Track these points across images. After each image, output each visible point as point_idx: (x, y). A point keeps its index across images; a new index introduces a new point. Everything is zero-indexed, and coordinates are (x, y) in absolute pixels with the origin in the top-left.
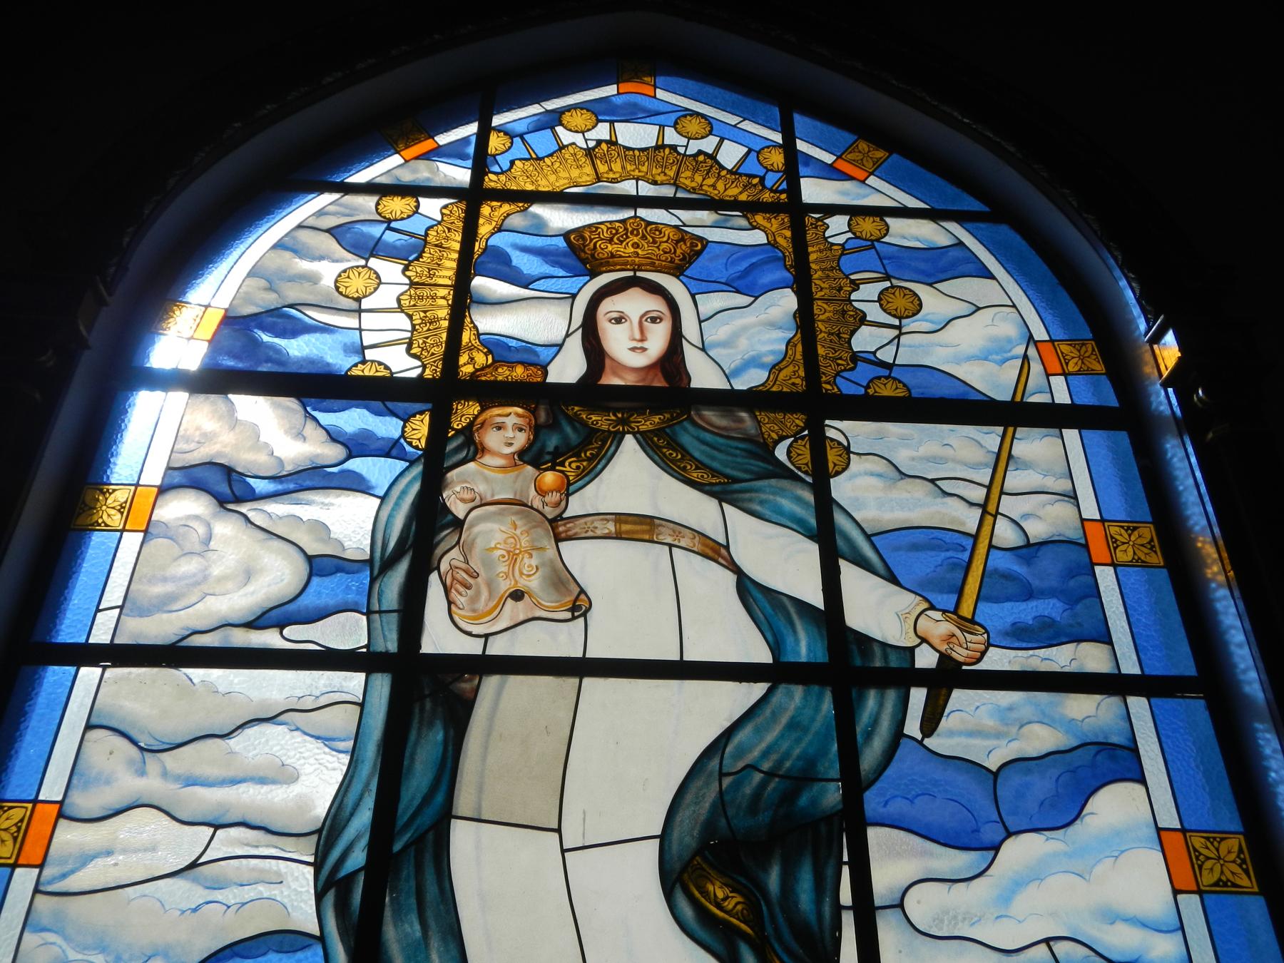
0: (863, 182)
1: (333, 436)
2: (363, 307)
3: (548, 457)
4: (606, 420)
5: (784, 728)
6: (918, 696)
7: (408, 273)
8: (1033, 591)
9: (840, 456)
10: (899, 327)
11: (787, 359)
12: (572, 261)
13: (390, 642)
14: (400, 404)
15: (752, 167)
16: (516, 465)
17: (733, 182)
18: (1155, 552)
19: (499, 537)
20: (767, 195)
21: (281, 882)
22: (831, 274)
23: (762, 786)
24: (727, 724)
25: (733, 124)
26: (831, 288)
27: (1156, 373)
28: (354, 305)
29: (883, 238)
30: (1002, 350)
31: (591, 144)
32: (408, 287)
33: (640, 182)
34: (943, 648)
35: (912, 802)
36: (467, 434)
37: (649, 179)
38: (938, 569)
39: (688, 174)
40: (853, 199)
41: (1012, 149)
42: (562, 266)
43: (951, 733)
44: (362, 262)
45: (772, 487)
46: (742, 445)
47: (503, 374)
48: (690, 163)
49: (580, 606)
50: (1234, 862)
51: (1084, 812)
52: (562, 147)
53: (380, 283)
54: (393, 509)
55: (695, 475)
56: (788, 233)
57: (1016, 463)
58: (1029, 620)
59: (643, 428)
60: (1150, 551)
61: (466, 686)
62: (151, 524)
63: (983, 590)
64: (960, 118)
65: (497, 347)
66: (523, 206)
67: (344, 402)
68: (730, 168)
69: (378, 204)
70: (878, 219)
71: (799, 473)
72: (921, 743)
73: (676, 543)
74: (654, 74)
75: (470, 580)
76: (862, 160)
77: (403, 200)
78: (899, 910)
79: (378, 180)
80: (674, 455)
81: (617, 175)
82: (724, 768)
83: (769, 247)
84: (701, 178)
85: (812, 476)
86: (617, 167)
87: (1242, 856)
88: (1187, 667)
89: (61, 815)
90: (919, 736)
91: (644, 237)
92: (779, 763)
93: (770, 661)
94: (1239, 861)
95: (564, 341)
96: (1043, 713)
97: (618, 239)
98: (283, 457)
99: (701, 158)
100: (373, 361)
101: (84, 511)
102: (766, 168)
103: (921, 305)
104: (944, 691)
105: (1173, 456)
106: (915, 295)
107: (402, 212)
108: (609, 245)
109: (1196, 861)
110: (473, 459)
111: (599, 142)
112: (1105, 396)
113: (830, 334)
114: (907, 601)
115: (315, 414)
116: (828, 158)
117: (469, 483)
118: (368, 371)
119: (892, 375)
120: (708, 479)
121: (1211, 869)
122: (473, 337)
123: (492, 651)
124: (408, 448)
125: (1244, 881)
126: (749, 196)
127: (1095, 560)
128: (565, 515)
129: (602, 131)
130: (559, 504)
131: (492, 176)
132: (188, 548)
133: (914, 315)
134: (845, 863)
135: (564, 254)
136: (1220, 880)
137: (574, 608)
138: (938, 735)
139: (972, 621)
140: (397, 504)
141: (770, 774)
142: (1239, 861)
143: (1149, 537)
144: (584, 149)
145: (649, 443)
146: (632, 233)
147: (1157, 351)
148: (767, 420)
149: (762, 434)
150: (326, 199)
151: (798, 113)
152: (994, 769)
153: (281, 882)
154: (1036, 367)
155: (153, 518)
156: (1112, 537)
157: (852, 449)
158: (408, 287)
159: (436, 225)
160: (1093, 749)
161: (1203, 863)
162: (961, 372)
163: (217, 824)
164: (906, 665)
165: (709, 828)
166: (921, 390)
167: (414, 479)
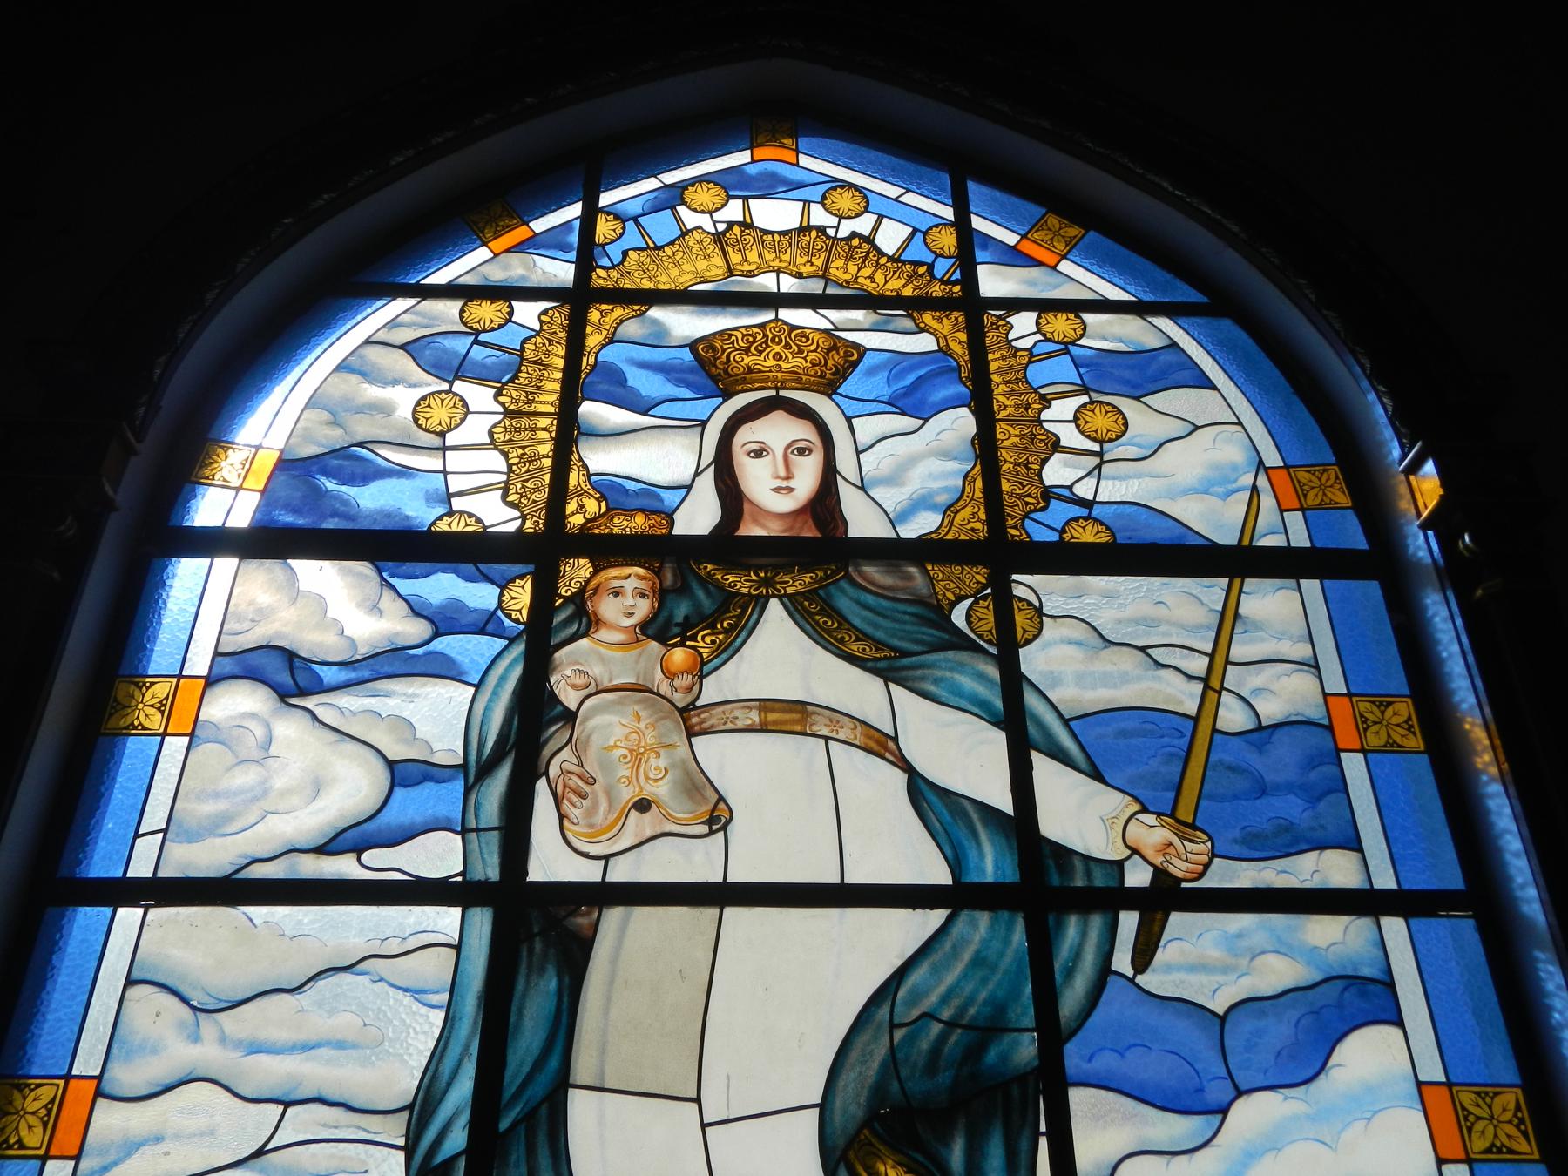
0: (1054, 268)
1: (415, 608)
3: (676, 630)
4: (746, 581)
5: (967, 966)
6: (1129, 921)
7: (501, 399)
8: (1266, 787)
9: (1030, 619)
10: (1100, 454)
11: (965, 497)
13: (490, 870)
14: (496, 566)
15: (917, 252)
16: (638, 641)
17: (895, 272)
18: (1414, 733)
19: (619, 732)
20: (937, 288)
21: (366, 1171)
22: (1015, 387)
23: (942, 1039)
24: (898, 963)
25: (894, 197)
26: (1017, 406)
27: (1413, 511)
30: (1225, 480)
31: (721, 227)
32: (502, 416)
34: (1158, 860)
35: (1122, 1055)
36: (578, 602)
37: (792, 271)
38: (1151, 762)
39: (840, 263)
40: (1042, 291)
41: (1235, 229)
42: (689, 385)
43: (1169, 968)
44: (445, 386)
47: (620, 525)
50: (1510, 1122)
51: (1330, 1064)
52: (685, 233)
53: (468, 412)
54: (490, 700)
55: (855, 649)
56: (963, 337)
57: (1245, 623)
59: (791, 590)
60: (1407, 732)
61: (583, 921)
63: (1205, 786)
64: (1170, 189)
65: (612, 491)
66: (639, 309)
67: (427, 566)
68: (891, 253)
69: (462, 311)
70: (1072, 316)
71: (982, 643)
72: (1132, 981)
73: (833, 735)
74: (794, 134)
75: (586, 788)
76: (1052, 239)
77: (494, 305)
79: (462, 281)
80: (830, 623)
81: (753, 267)
82: (895, 1017)
83: (940, 354)
85: (997, 645)
86: (753, 256)
87: (1520, 1115)
88: (1451, 877)
90: (1130, 972)
91: (787, 346)
92: (962, 1010)
93: (950, 882)
96: (1279, 940)
98: (355, 637)
99: (855, 242)
100: (461, 513)
101: (116, 711)
102: (935, 252)
103: (1126, 425)
104: (1159, 916)
105: (1435, 615)
106: (1120, 412)
107: (492, 321)
108: (744, 356)
109: (1465, 1122)
110: (586, 634)
111: (730, 225)
112: (1352, 536)
113: (1016, 464)
114: (1114, 803)
115: (393, 581)
117: (579, 663)
118: (457, 525)
120: (871, 653)
121: (1483, 1132)
122: (582, 478)
123: (613, 877)
124: (507, 622)
125: (1523, 1146)
126: (914, 290)
127: (1341, 746)
128: (698, 703)
129: (734, 211)
130: (692, 688)
132: (243, 755)
133: (1118, 437)
134: (1043, 1134)
135: (691, 370)
136: (1493, 1145)
137: (711, 821)
138: (1153, 971)
140: (495, 693)
141: (951, 1025)
142: (1516, 1121)
143: (1406, 715)
144: (712, 234)
145: (798, 609)
146: (773, 340)
147: (1414, 483)
148: (941, 575)
149: (936, 594)
150: (401, 304)
151: (973, 181)
152: (1221, 1012)
153: (366, 1171)
154: (1268, 501)
155: (200, 718)
156: (1362, 716)
158: (501, 416)
159: (534, 336)
160: (1340, 984)
161: (1473, 1124)
162: (1178, 509)
163: (287, 1100)
164: (1112, 883)
165: (878, 1092)
166: (1128, 534)
167: (515, 660)
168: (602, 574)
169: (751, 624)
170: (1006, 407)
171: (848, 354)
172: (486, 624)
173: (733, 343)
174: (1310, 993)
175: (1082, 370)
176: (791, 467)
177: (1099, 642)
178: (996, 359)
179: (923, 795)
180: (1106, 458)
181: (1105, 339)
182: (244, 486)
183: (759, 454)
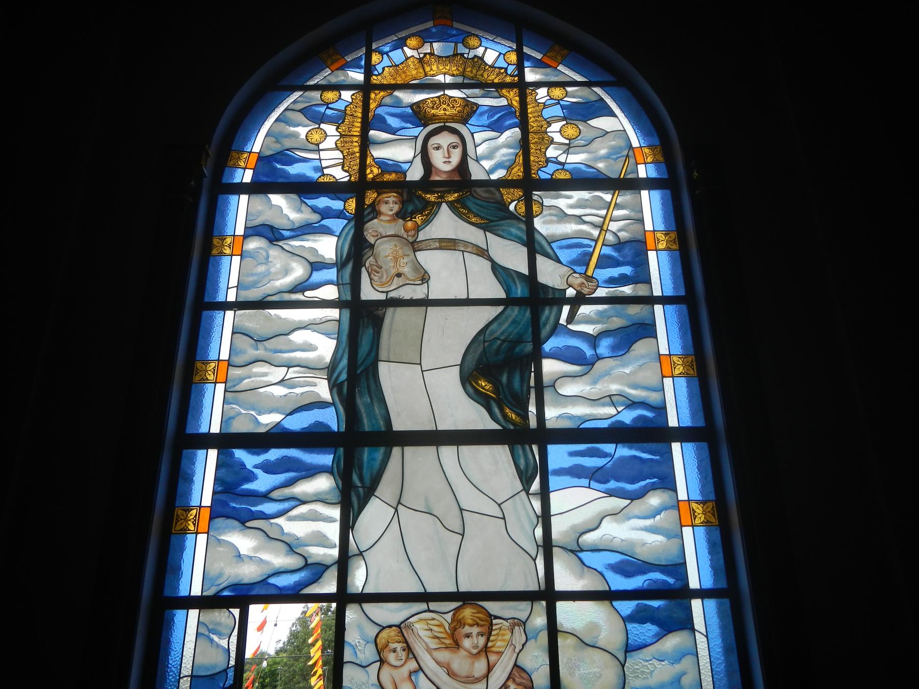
2: (320, 148)
6: (566, 309)
7: (339, 130)
12: (415, 119)
13: (348, 297)
15: (501, 63)
17: (491, 72)
19: (390, 251)
22: (538, 119)
23: (501, 345)
28: (316, 148)
31: (422, 56)
32: (339, 137)
33: (446, 76)
34: (579, 289)
42: (411, 123)
44: (317, 126)
46: (494, 205)
47: (387, 177)
48: (470, 63)
49: (425, 279)
52: (407, 58)
53: (327, 136)
54: (343, 241)
55: (474, 220)
56: (517, 98)
58: (616, 275)
61: (380, 312)
65: (382, 164)
68: (490, 64)
69: (321, 96)
73: (466, 250)
76: (556, 56)
78: (552, 388)
86: (434, 68)
89: (229, 365)
91: (448, 105)
92: (509, 336)
93: (505, 297)
97: (436, 106)
99: (476, 60)
100: (327, 175)
102: (508, 63)
110: (376, 218)
111: (425, 54)
117: (373, 228)
118: (326, 180)
119: (565, 168)
120: (479, 221)
122: (371, 160)
124: (347, 214)
128: (417, 240)
129: (427, 49)
130: (415, 235)
132: (260, 262)
133: (576, 137)
134: (533, 372)
135: (411, 116)
137: (422, 280)
139: (592, 277)
141: (504, 341)
142: (691, 365)
144: (418, 59)
145: (452, 206)
149: (504, 199)
150: (297, 95)
154: (632, 160)
155: (243, 249)
156: (657, 238)
157: (544, 204)
158: (339, 137)
159: (350, 105)
165: (479, 361)
167: (351, 227)
169: (436, 212)
170: (533, 127)
172: (339, 215)
174: (626, 329)
175: (564, 111)
176: (450, 153)
177: (563, 214)
180: (571, 146)
181: (574, 97)
183: (438, 148)
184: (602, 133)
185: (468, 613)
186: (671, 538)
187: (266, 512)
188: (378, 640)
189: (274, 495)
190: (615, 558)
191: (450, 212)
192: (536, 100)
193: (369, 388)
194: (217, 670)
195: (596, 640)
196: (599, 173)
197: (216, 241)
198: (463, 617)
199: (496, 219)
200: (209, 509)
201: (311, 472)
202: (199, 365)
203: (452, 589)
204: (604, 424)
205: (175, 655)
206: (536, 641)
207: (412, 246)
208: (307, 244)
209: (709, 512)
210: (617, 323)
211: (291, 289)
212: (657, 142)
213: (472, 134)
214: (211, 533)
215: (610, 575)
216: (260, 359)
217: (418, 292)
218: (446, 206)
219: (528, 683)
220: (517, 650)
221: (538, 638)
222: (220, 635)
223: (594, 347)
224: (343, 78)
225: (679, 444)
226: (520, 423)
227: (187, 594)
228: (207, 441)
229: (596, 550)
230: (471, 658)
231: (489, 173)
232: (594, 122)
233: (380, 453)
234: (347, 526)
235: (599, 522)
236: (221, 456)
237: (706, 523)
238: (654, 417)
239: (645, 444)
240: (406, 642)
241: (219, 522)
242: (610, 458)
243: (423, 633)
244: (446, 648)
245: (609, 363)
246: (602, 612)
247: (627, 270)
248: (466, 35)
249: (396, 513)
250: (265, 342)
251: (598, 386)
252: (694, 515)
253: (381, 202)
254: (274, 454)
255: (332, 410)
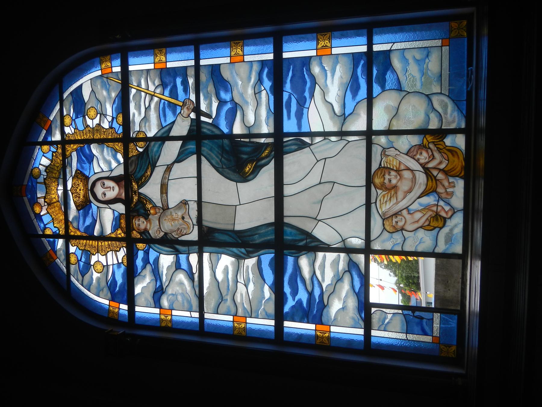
1: (144, 267)
2: (106, 265)
6: (203, 119)
7: (94, 253)
12: (87, 208)
13: (196, 247)
15: (49, 155)
16: (149, 220)
19: (169, 223)
23: (225, 158)
28: (105, 268)
29: (71, 117)
31: (46, 204)
32: (99, 254)
33: (58, 189)
44: (92, 267)
45: (151, 152)
46: (140, 161)
47: (123, 225)
48: (50, 175)
49: (185, 202)
51: (227, 80)
52: (48, 213)
53: (98, 261)
54: (163, 251)
55: (149, 173)
56: (72, 145)
58: (182, 87)
61: (205, 229)
62: (170, 309)
65: (115, 228)
68: (50, 162)
69: (73, 264)
71: (147, 145)
72: (213, 119)
73: (167, 178)
81: (57, 196)
84: (55, 171)
89: (236, 315)
91: (77, 188)
92: (219, 154)
93: (196, 155)
94: (237, 44)
95: (112, 209)
97: (78, 195)
99: (48, 171)
100: (122, 260)
102: (49, 151)
111: (45, 202)
115: (138, 274)
116: (44, 132)
117: (155, 233)
118: (125, 261)
122: (113, 234)
124: (146, 248)
126: (60, 156)
128: (162, 207)
129: (42, 201)
131: (61, 233)
133: (96, 109)
135: (85, 210)
139: (183, 102)
141: (222, 156)
143: (158, 51)
149: (136, 155)
150: (73, 279)
155: (168, 309)
156: (159, 61)
157: (139, 130)
159: (78, 247)
165: (234, 171)
167: (154, 246)
168: (134, 228)
170: (90, 136)
171: (78, 173)
173: (77, 201)
174: (215, 82)
175: (79, 117)
176: (108, 187)
177: (145, 118)
178: (78, 137)
179: (179, 160)
182: (118, 307)
183: (105, 194)
184: (93, 94)
185: (377, 181)
186: (338, 61)
187: (319, 294)
188: (391, 231)
189: (310, 289)
190: (349, 94)
191: (144, 187)
192: (73, 134)
193: (250, 236)
194: (404, 319)
195: (394, 108)
196: (118, 96)
197: (163, 325)
198: (380, 183)
199: (148, 160)
200: (317, 325)
201: (297, 268)
202: (236, 332)
203: (364, 190)
204: (272, 98)
205: (395, 343)
206: (394, 142)
207: (166, 210)
208: (165, 272)
209: (323, 37)
210: (211, 88)
211: (192, 281)
212: (98, 59)
213: (95, 173)
214: (330, 324)
215: (359, 98)
216: (233, 298)
217: (193, 207)
218: (140, 190)
219: (417, 148)
220: (399, 153)
221: (392, 141)
222: (385, 318)
223: (225, 102)
224: (61, 252)
225: (284, 54)
226: (271, 148)
227: (363, 337)
228: (279, 326)
229: (344, 106)
230: (402, 179)
231: (119, 163)
232: (86, 98)
233: (287, 230)
234: (328, 248)
235: (328, 103)
236: (288, 319)
237: (330, 40)
238: (267, 68)
239: (284, 74)
240: (392, 216)
241: (324, 319)
242: (292, 95)
243: (388, 206)
244: (396, 194)
245: (235, 93)
246: (379, 104)
247: (179, 81)
248: (32, 176)
249: (321, 221)
250: (223, 296)
251: (249, 100)
252: (325, 47)
253: (138, 229)
254: (287, 289)
255: (262, 257)
